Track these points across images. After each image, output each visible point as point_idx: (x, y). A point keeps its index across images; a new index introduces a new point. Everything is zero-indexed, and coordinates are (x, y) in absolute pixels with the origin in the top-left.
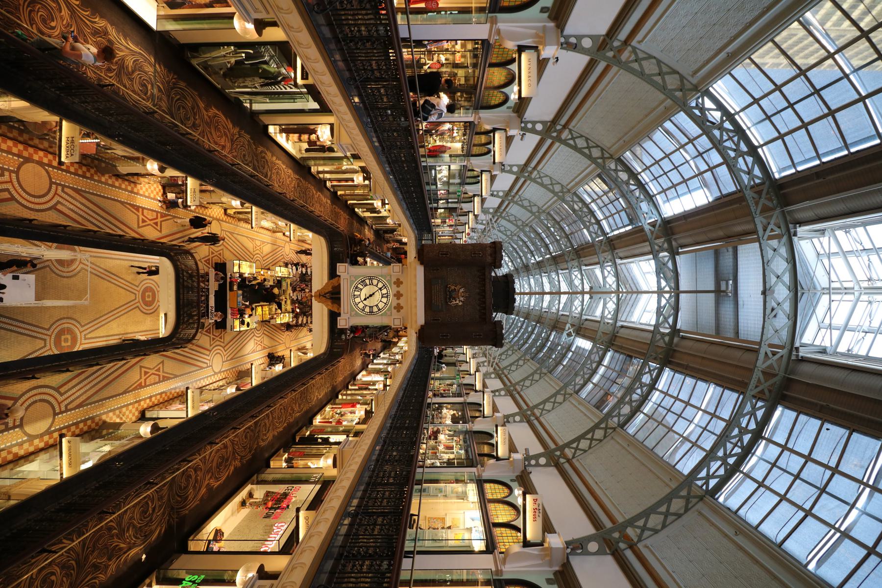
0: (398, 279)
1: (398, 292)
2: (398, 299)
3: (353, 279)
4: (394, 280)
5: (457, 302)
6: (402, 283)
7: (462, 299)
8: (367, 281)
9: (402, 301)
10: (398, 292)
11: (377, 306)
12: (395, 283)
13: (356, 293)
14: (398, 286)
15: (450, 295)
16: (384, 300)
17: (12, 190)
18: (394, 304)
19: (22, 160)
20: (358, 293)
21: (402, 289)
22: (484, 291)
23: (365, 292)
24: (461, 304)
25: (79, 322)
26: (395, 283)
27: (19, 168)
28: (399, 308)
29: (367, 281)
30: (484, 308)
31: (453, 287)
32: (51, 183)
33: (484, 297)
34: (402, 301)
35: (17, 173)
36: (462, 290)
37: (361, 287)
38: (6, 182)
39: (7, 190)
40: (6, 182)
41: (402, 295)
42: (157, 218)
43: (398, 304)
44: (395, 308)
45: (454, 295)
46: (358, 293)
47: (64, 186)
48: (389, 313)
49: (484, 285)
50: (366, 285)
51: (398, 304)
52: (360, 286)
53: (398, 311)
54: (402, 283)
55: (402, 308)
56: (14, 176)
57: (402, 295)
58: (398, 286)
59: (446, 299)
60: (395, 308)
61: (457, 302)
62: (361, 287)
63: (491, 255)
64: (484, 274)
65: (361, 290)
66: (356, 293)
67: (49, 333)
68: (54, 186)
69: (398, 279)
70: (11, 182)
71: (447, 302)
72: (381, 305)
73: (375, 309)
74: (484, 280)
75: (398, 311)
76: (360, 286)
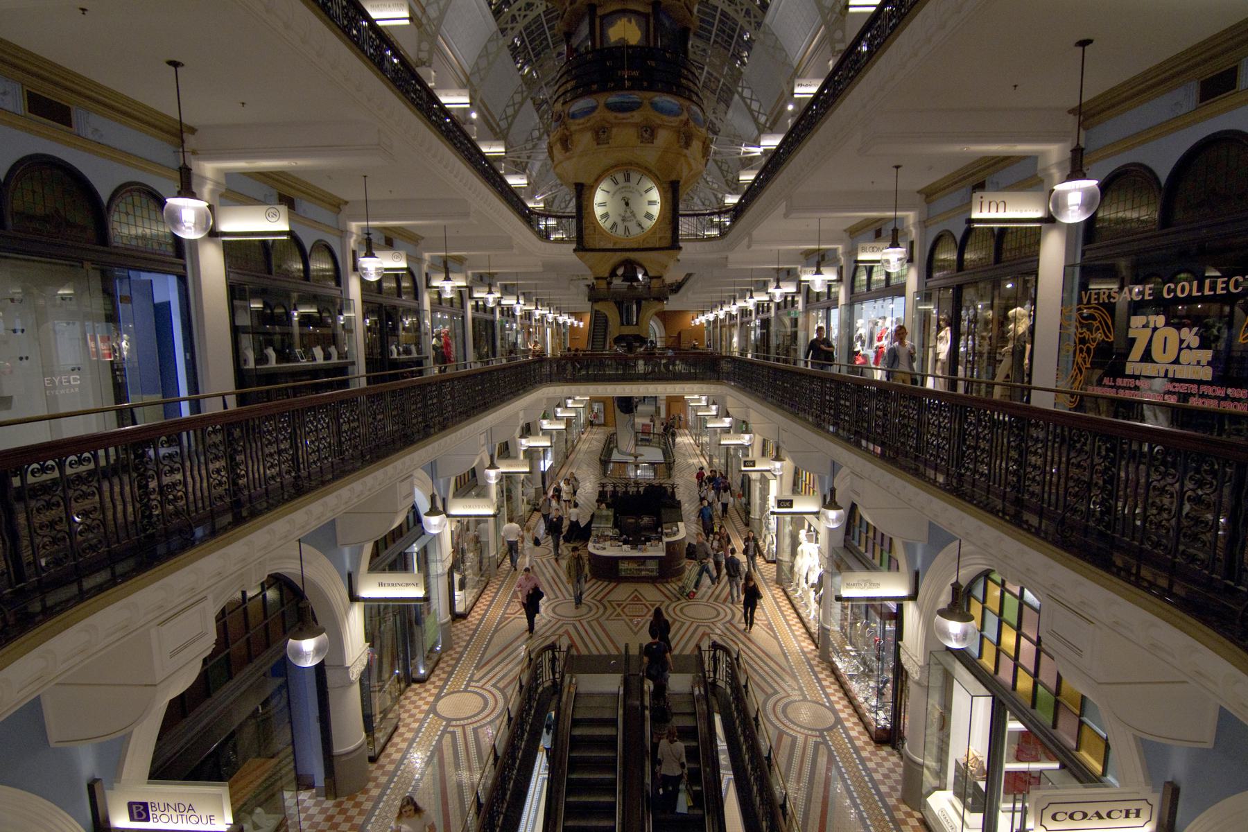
17: (475, 725)
19: (431, 716)
27: (445, 719)
32: (465, 690)
35: (449, 720)
47: (471, 679)
56: (454, 723)
68: (469, 689)
70: (463, 726)
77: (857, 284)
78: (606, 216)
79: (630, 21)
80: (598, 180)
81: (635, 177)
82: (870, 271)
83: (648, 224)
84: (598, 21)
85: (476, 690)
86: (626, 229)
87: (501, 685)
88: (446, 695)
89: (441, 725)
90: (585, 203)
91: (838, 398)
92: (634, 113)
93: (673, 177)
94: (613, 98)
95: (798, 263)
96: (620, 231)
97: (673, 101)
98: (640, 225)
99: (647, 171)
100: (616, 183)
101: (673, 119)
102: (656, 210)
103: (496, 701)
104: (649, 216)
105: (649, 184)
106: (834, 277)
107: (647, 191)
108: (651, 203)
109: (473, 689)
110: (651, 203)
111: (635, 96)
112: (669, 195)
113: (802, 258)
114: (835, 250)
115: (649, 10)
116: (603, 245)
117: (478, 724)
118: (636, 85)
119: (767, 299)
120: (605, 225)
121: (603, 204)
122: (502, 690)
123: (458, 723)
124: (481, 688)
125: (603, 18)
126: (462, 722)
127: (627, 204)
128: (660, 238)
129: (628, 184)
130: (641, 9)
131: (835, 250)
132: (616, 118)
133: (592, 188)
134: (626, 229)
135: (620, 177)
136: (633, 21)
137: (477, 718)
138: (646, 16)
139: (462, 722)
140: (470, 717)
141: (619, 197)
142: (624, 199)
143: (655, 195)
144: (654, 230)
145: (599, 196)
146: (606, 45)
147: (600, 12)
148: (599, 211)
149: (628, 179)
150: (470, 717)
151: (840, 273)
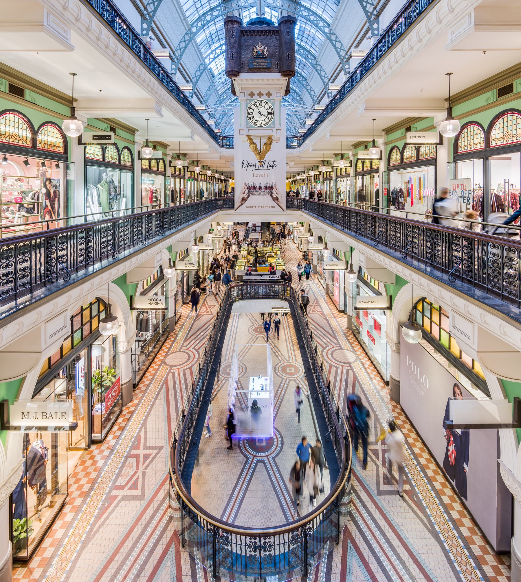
0: (249, 95)
1: (258, 95)
2: (263, 95)
3: (248, 126)
4: (249, 97)
5: (265, 50)
6: (252, 92)
7: (263, 47)
8: (251, 116)
9: (264, 92)
10: (258, 95)
11: (267, 110)
12: (252, 97)
13: (258, 123)
14: (254, 95)
15: (260, 56)
16: (263, 104)
17: (184, 368)
18: (266, 97)
20: (259, 122)
21: (256, 92)
22: (258, 31)
23: (257, 117)
24: (266, 48)
25: (278, 364)
26: (252, 97)
27: (169, 365)
28: (269, 94)
29: (251, 116)
30: (270, 31)
31: (255, 53)
33: (262, 31)
34: (264, 92)
35: (172, 366)
36: (258, 48)
37: (254, 120)
38: (179, 371)
39: (184, 371)
40: (179, 371)
41: (260, 92)
42: (207, 309)
43: (266, 94)
44: (269, 97)
45: (260, 53)
46: (259, 122)
48: (272, 101)
49: (254, 31)
50: (253, 117)
51: (266, 94)
52: (254, 121)
53: (271, 95)
54: (252, 92)
55: (269, 92)
56: (173, 368)
57: (260, 92)
58: (254, 95)
59: (262, 58)
60: (269, 97)
61: (265, 50)
62: (254, 120)
63: (233, 24)
64: (246, 32)
65: (256, 120)
66: (258, 123)
67: (285, 378)
69: (249, 95)
70: (178, 369)
71: (265, 58)
72: (267, 106)
73: (270, 111)
74: (250, 31)
75: (271, 95)
76: (254, 121)
77: (358, 168)
82: (363, 163)
85: (185, 351)
87: (197, 348)
88: (171, 354)
89: (167, 369)
91: (351, 218)
95: (332, 158)
103: (194, 355)
106: (348, 165)
109: (183, 350)
113: (333, 156)
114: (348, 153)
117: (186, 368)
119: (318, 173)
122: (197, 350)
123: (175, 368)
124: (187, 349)
126: (177, 367)
131: (348, 153)
137: (184, 365)
139: (177, 367)
140: (181, 365)
150: (181, 365)
151: (351, 163)
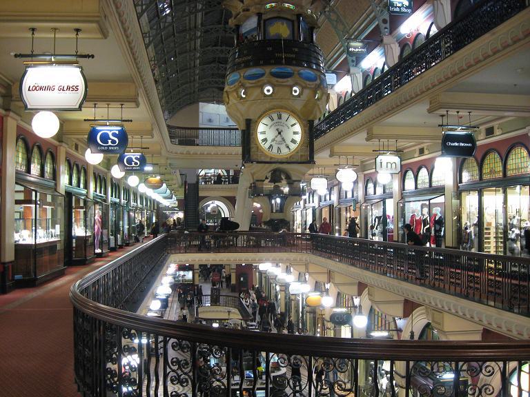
78: (265, 140)
79: (283, 24)
80: (260, 117)
81: (285, 116)
83: (293, 147)
84: (262, 22)
86: (279, 149)
90: (251, 132)
92: (289, 79)
93: (311, 118)
94: (275, 69)
96: (275, 150)
97: (312, 73)
98: (288, 147)
99: (293, 112)
100: (272, 120)
101: (311, 83)
102: (298, 138)
104: (293, 141)
105: (293, 120)
107: (292, 126)
108: (295, 133)
110: (295, 133)
111: (289, 69)
112: (307, 129)
115: (294, 18)
116: (263, 159)
118: (289, 62)
120: (266, 146)
121: (264, 133)
125: (265, 21)
127: (280, 133)
128: (301, 156)
129: (280, 121)
130: (289, 17)
132: (277, 81)
133: (257, 122)
134: (279, 149)
135: (275, 116)
136: (285, 25)
138: (293, 21)
141: (274, 128)
142: (277, 130)
143: (298, 128)
144: (297, 151)
145: (261, 128)
146: (267, 38)
147: (264, 17)
148: (260, 137)
149: (280, 118)
